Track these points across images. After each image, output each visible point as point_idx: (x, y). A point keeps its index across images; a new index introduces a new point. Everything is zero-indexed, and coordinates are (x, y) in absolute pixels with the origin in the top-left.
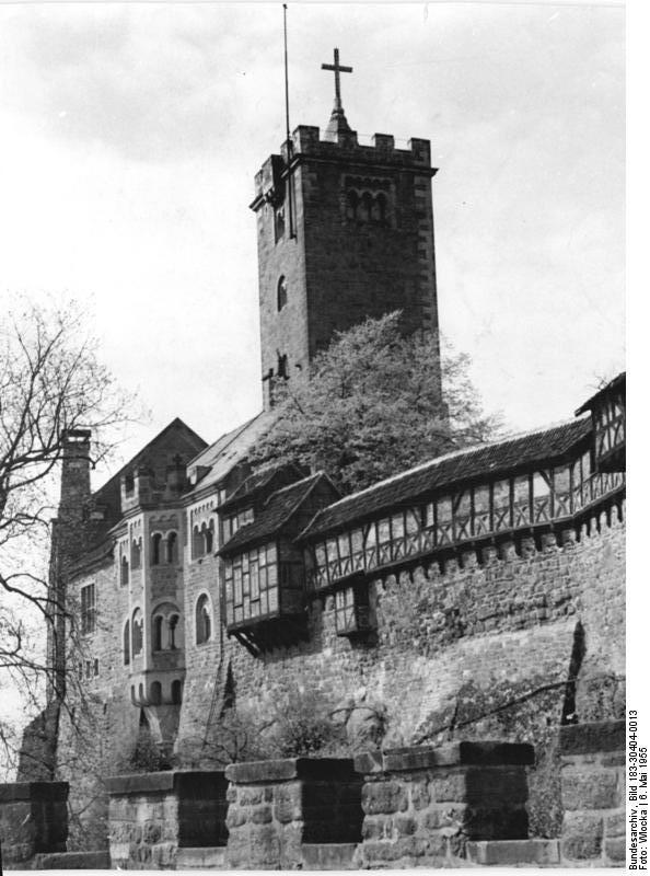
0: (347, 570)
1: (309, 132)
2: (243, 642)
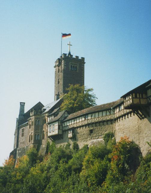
0: (72, 127)
1: (65, 55)
2: (50, 139)
